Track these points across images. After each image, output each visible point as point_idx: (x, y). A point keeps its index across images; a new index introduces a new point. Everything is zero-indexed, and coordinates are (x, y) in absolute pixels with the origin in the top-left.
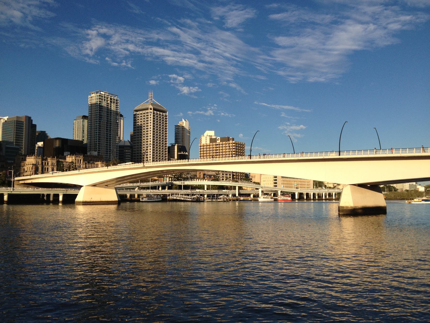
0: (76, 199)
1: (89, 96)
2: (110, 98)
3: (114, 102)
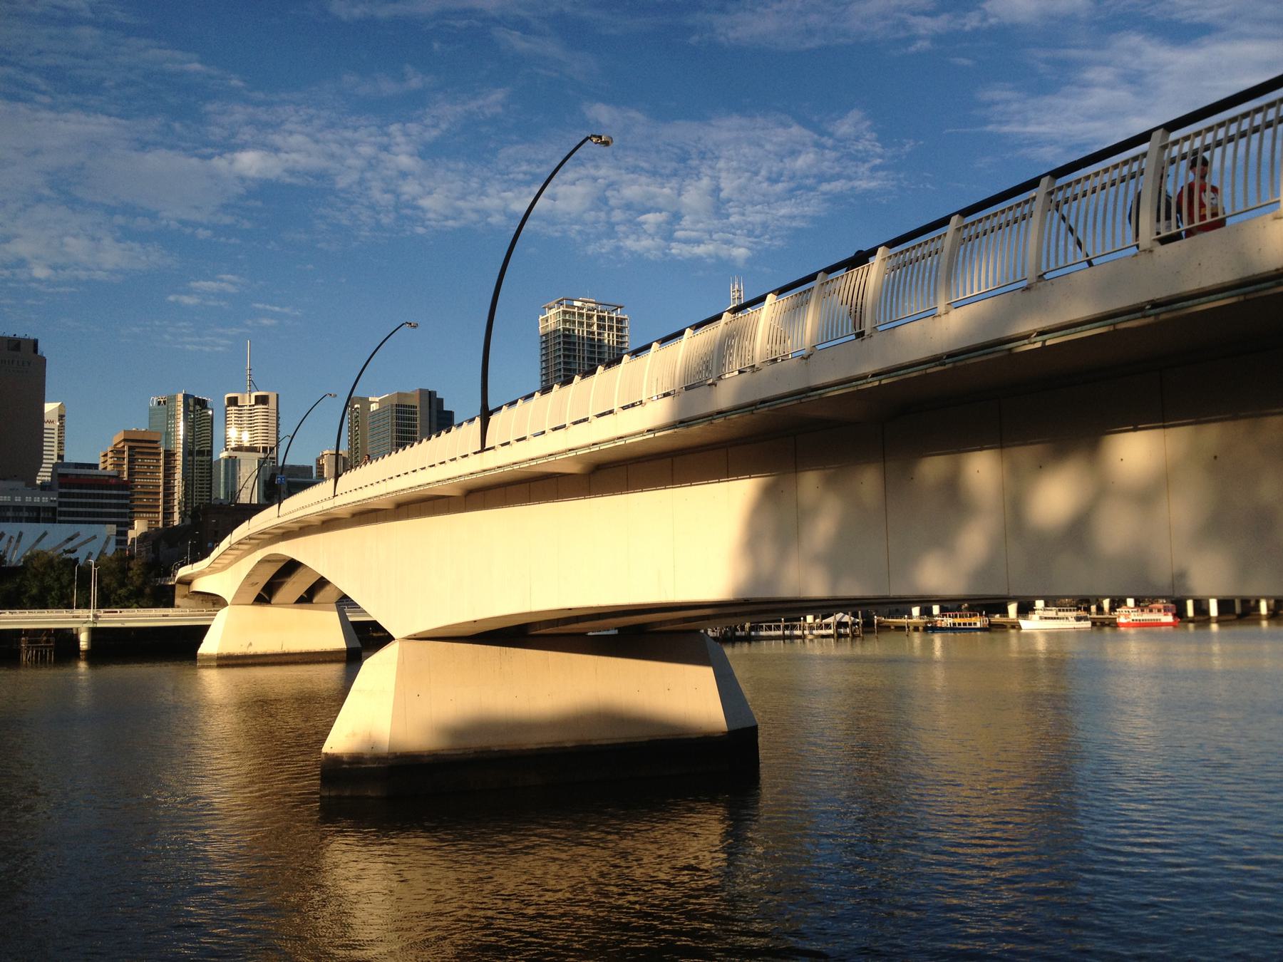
0: (199, 646)
2: (599, 317)
3: (611, 328)
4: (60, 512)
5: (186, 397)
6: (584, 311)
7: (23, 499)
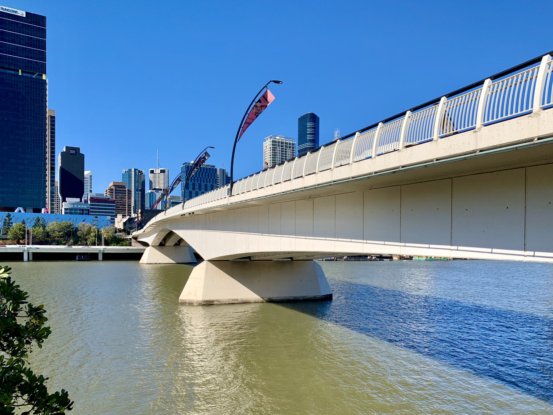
1: (264, 143)
3: (290, 147)
4: (91, 211)
5: (135, 170)
6: (280, 140)
7: (77, 206)
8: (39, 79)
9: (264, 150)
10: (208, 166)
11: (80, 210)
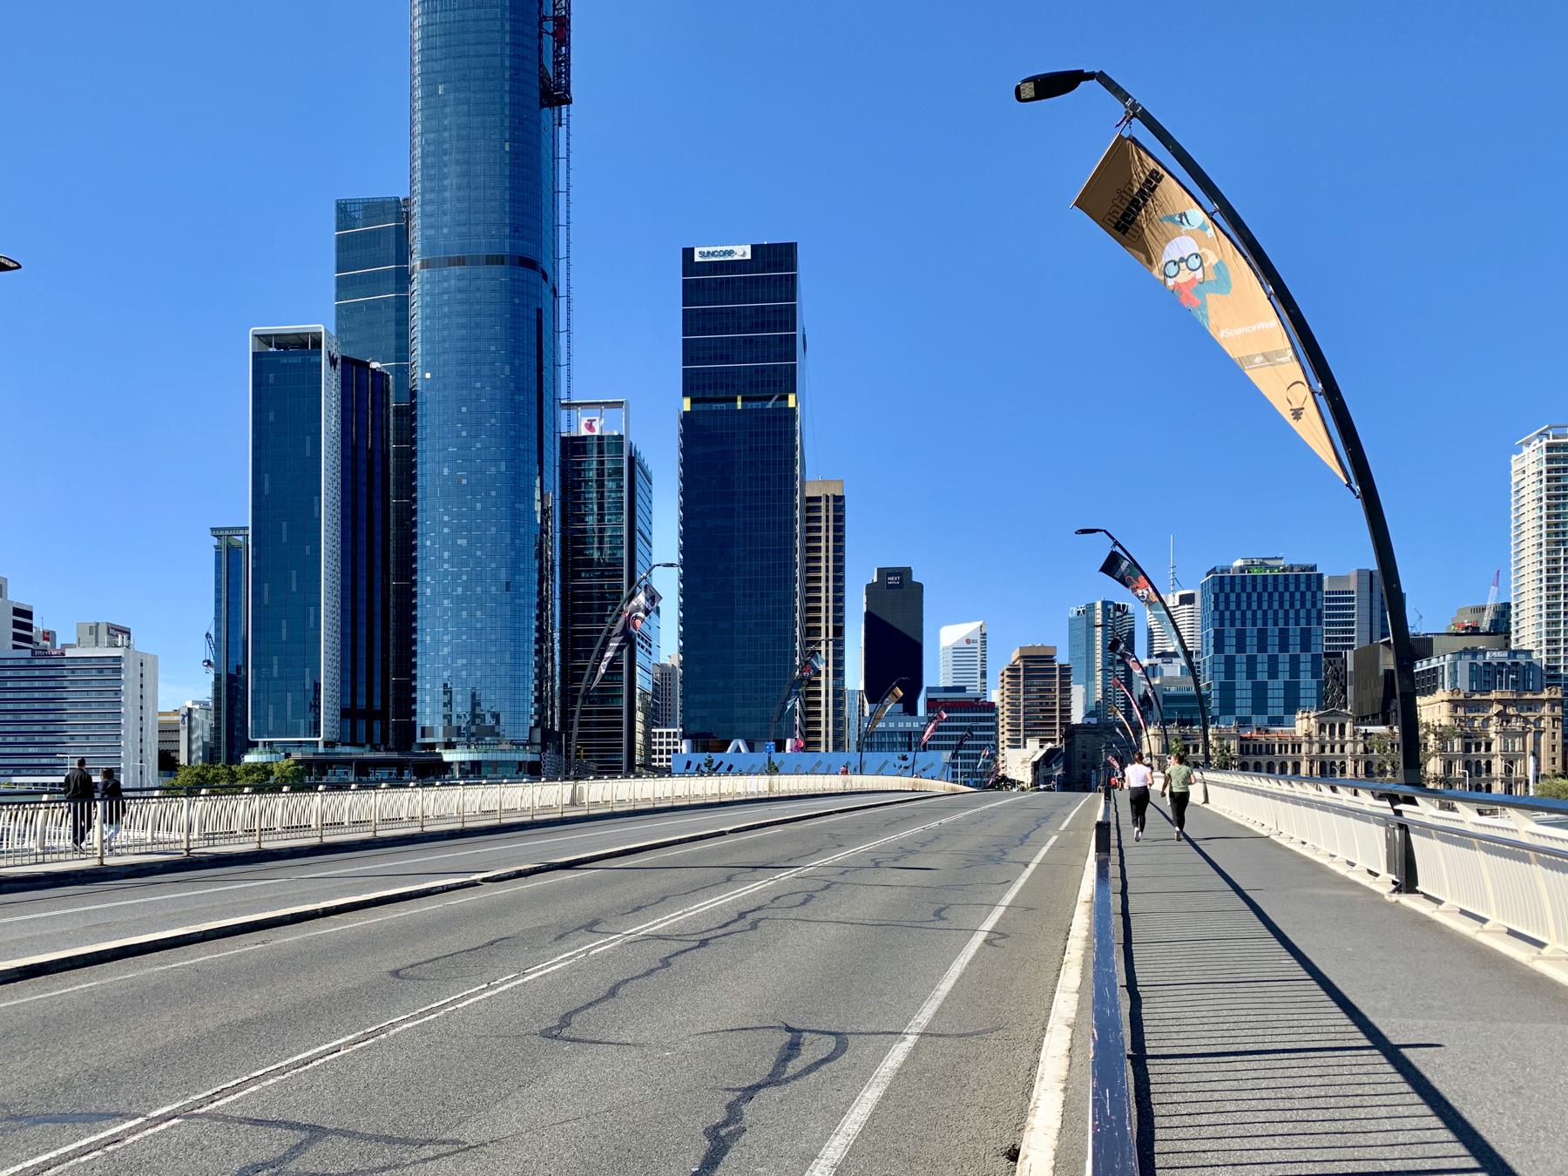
1: (1514, 457)
5: (1105, 604)
7: (896, 725)
8: (780, 409)
9: (1517, 483)
10: (1292, 568)
11: (903, 734)
